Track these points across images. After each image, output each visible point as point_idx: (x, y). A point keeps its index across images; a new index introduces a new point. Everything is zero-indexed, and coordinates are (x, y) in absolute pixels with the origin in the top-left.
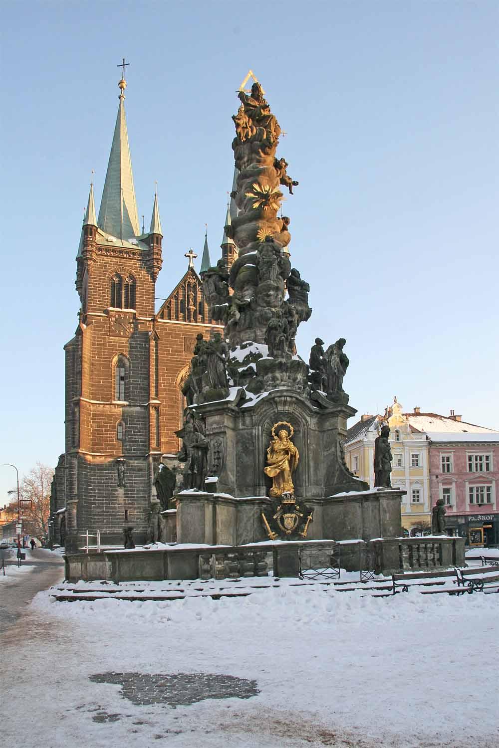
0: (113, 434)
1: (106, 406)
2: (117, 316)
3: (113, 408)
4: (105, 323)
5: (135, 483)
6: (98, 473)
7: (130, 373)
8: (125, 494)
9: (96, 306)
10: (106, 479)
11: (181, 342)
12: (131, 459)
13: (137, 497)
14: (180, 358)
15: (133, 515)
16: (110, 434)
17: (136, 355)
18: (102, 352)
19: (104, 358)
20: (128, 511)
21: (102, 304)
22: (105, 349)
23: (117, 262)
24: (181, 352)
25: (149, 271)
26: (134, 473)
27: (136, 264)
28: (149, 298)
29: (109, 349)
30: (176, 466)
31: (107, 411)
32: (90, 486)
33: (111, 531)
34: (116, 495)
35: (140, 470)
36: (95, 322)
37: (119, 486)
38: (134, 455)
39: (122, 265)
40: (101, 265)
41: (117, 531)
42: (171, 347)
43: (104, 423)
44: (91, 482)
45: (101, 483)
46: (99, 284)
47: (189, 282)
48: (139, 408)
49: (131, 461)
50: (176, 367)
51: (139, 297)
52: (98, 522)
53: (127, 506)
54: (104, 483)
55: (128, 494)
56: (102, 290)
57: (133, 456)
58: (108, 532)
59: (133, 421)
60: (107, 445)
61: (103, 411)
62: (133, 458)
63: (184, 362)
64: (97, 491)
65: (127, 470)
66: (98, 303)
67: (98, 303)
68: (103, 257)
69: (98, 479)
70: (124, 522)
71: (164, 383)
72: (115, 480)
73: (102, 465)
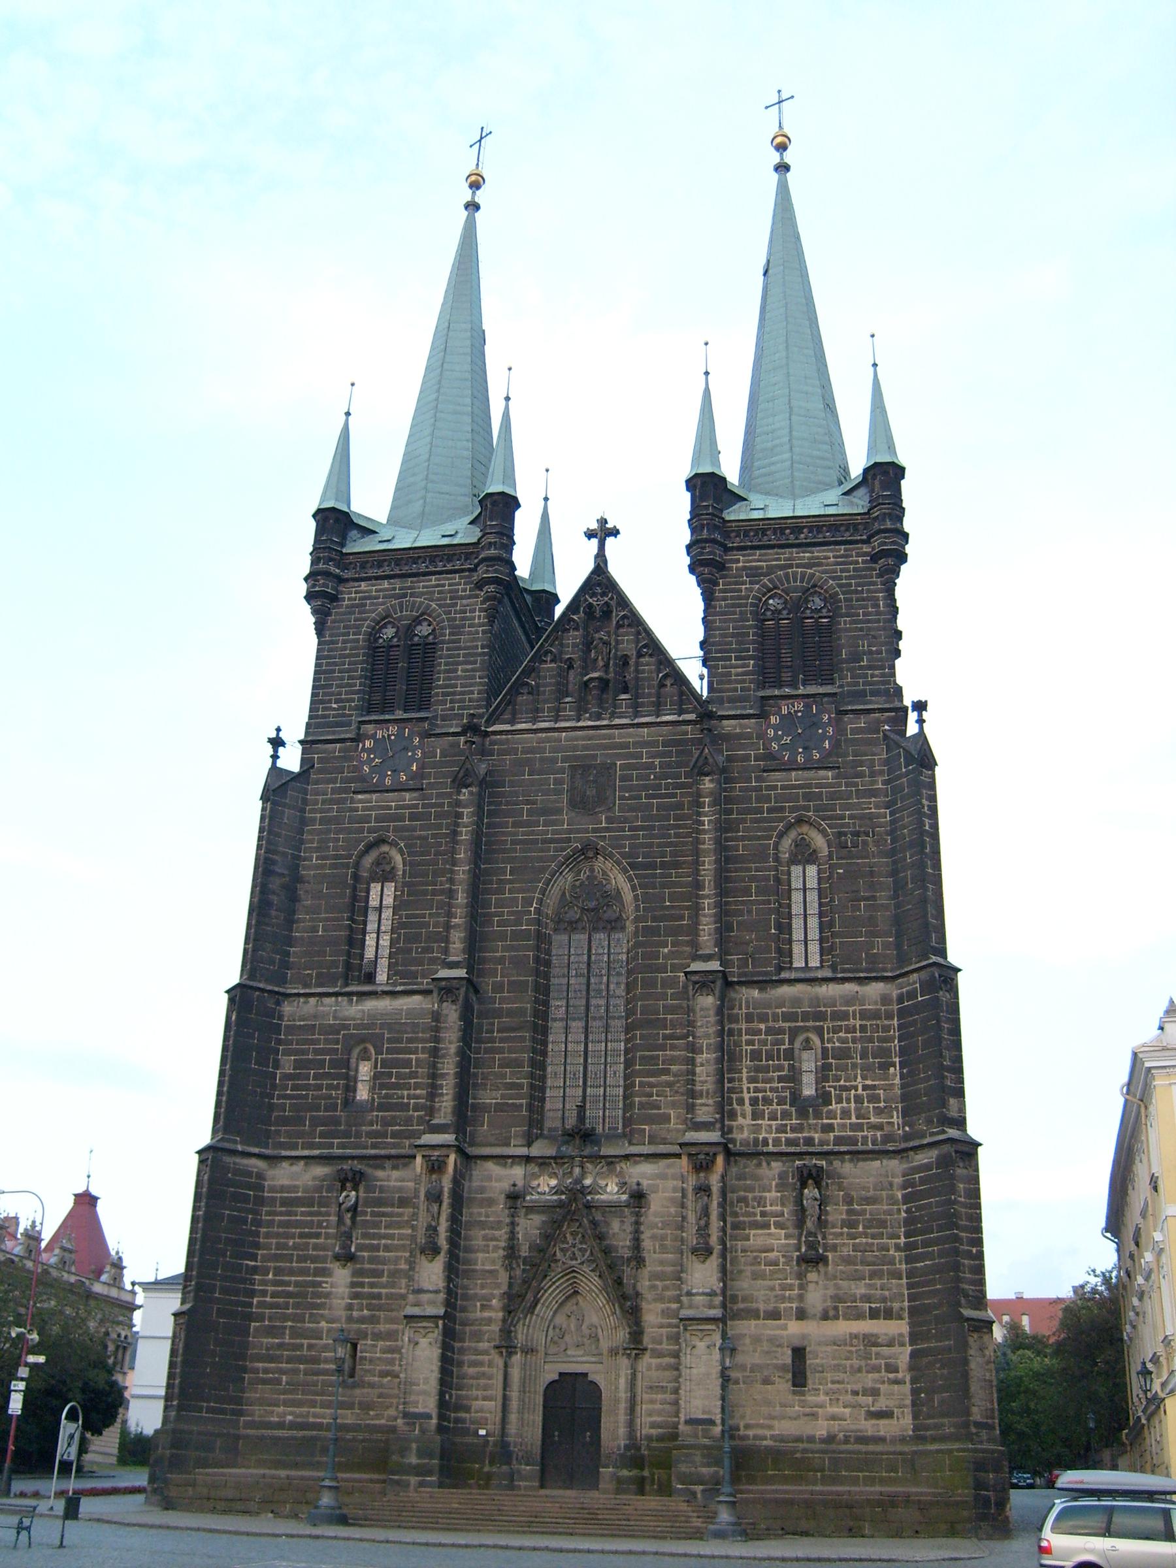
0: (337, 1088)
1: (327, 1000)
2: (379, 735)
3: (345, 1003)
4: (345, 759)
5: (387, 1248)
6: (281, 1214)
7: (403, 892)
8: (353, 1285)
9: (328, 716)
10: (301, 1236)
11: (558, 782)
12: (376, 1167)
13: (390, 1296)
14: (554, 832)
15: (371, 1361)
16: (329, 1087)
17: (426, 838)
18: (329, 840)
19: (336, 857)
20: (359, 1346)
21: (344, 708)
22: (338, 832)
23: (394, 589)
24: (559, 811)
25: (477, 596)
26: (384, 1214)
27: (444, 585)
28: (473, 670)
29: (349, 831)
30: (520, 1183)
31: (328, 1014)
32: (254, 1257)
33: (301, 1415)
34: (326, 1288)
35: (403, 1202)
36: (321, 760)
37: (337, 1258)
38: (393, 1152)
39: (405, 596)
40: (353, 606)
41: (315, 1416)
42: (528, 802)
43: (316, 1052)
44: (257, 1246)
45: (285, 1246)
46: (342, 656)
47: (590, 606)
48: (417, 998)
49: (380, 1174)
50: (541, 859)
51: (447, 671)
52: (265, 1382)
53: (355, 1326)
54: (295, 1247)
55: (362, 1285)
56: (348, 671)
57: (389, 1157)
58: (290, 1418)
59: (399, 1041)
60: (315, 1122)
61: (315, 1017)
62: (388, 1164)
63: (569, 840)
64: (270, 1276)
65: (369, 1203)
66: (335, 706)
67: (335, 706)
68: (356, 584)
69: (278, 1235)
70: (344, 1384)
71: (501, 914)
72: (327, 1236)
73: (294, 1189)
